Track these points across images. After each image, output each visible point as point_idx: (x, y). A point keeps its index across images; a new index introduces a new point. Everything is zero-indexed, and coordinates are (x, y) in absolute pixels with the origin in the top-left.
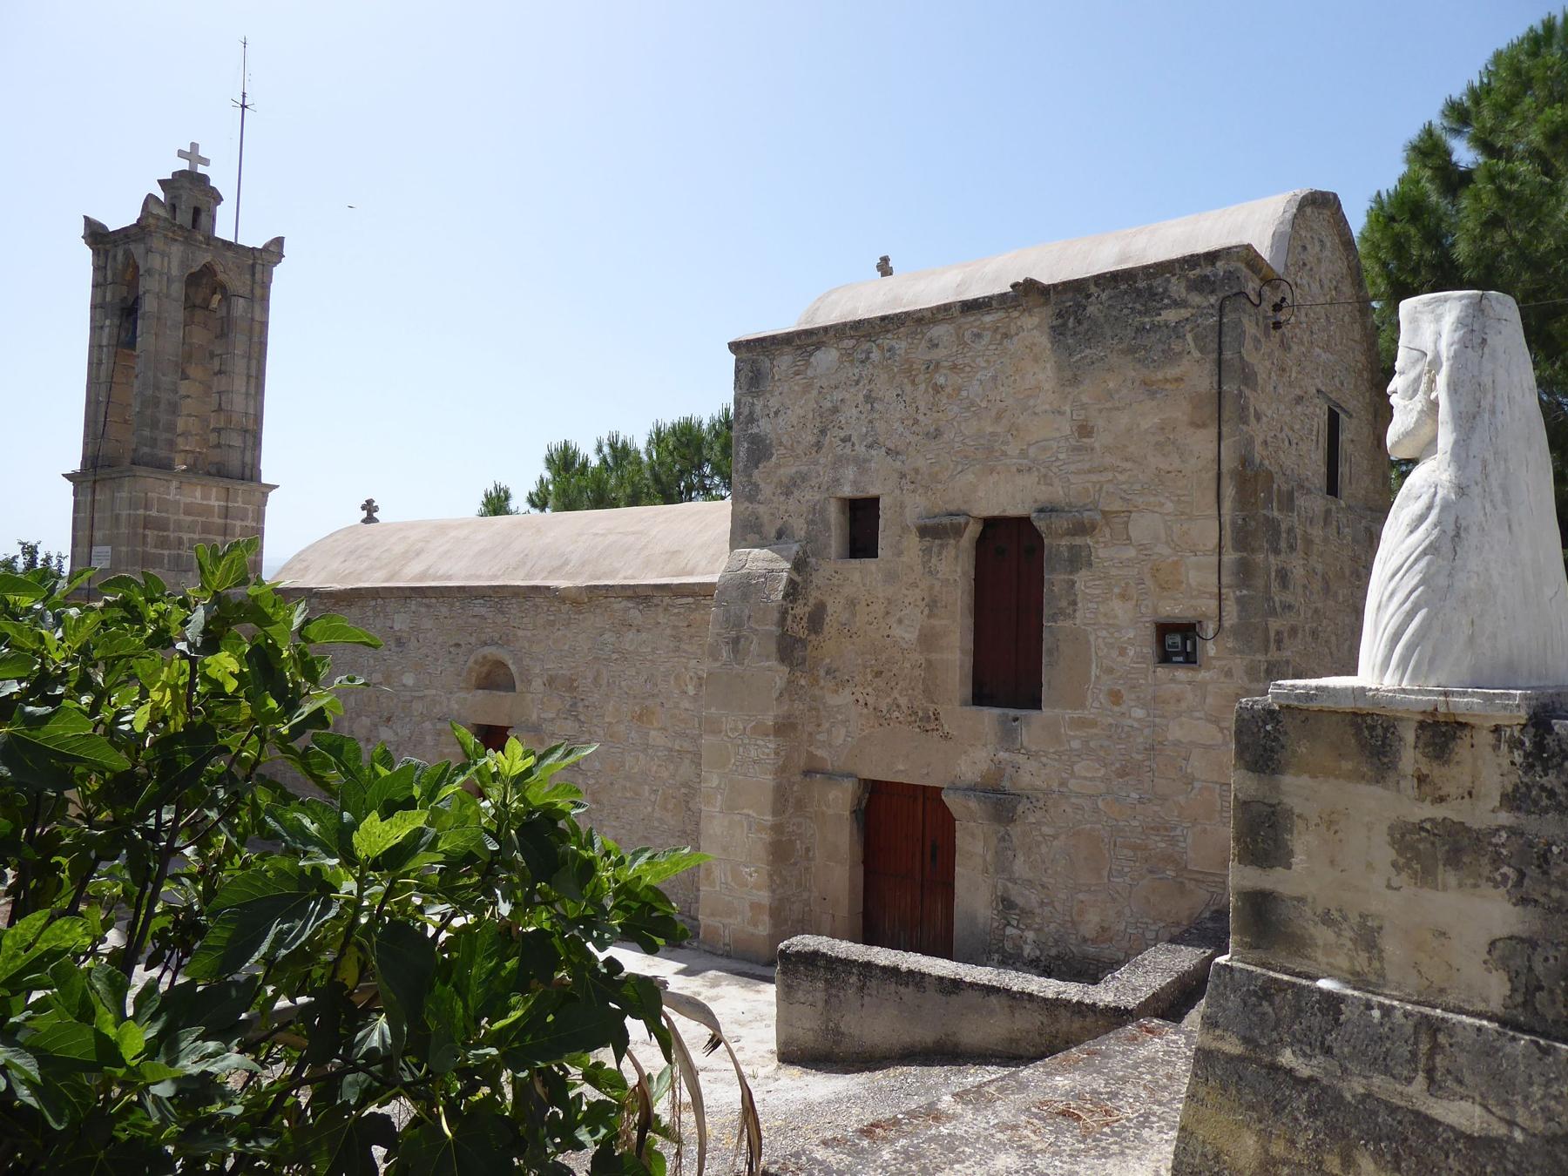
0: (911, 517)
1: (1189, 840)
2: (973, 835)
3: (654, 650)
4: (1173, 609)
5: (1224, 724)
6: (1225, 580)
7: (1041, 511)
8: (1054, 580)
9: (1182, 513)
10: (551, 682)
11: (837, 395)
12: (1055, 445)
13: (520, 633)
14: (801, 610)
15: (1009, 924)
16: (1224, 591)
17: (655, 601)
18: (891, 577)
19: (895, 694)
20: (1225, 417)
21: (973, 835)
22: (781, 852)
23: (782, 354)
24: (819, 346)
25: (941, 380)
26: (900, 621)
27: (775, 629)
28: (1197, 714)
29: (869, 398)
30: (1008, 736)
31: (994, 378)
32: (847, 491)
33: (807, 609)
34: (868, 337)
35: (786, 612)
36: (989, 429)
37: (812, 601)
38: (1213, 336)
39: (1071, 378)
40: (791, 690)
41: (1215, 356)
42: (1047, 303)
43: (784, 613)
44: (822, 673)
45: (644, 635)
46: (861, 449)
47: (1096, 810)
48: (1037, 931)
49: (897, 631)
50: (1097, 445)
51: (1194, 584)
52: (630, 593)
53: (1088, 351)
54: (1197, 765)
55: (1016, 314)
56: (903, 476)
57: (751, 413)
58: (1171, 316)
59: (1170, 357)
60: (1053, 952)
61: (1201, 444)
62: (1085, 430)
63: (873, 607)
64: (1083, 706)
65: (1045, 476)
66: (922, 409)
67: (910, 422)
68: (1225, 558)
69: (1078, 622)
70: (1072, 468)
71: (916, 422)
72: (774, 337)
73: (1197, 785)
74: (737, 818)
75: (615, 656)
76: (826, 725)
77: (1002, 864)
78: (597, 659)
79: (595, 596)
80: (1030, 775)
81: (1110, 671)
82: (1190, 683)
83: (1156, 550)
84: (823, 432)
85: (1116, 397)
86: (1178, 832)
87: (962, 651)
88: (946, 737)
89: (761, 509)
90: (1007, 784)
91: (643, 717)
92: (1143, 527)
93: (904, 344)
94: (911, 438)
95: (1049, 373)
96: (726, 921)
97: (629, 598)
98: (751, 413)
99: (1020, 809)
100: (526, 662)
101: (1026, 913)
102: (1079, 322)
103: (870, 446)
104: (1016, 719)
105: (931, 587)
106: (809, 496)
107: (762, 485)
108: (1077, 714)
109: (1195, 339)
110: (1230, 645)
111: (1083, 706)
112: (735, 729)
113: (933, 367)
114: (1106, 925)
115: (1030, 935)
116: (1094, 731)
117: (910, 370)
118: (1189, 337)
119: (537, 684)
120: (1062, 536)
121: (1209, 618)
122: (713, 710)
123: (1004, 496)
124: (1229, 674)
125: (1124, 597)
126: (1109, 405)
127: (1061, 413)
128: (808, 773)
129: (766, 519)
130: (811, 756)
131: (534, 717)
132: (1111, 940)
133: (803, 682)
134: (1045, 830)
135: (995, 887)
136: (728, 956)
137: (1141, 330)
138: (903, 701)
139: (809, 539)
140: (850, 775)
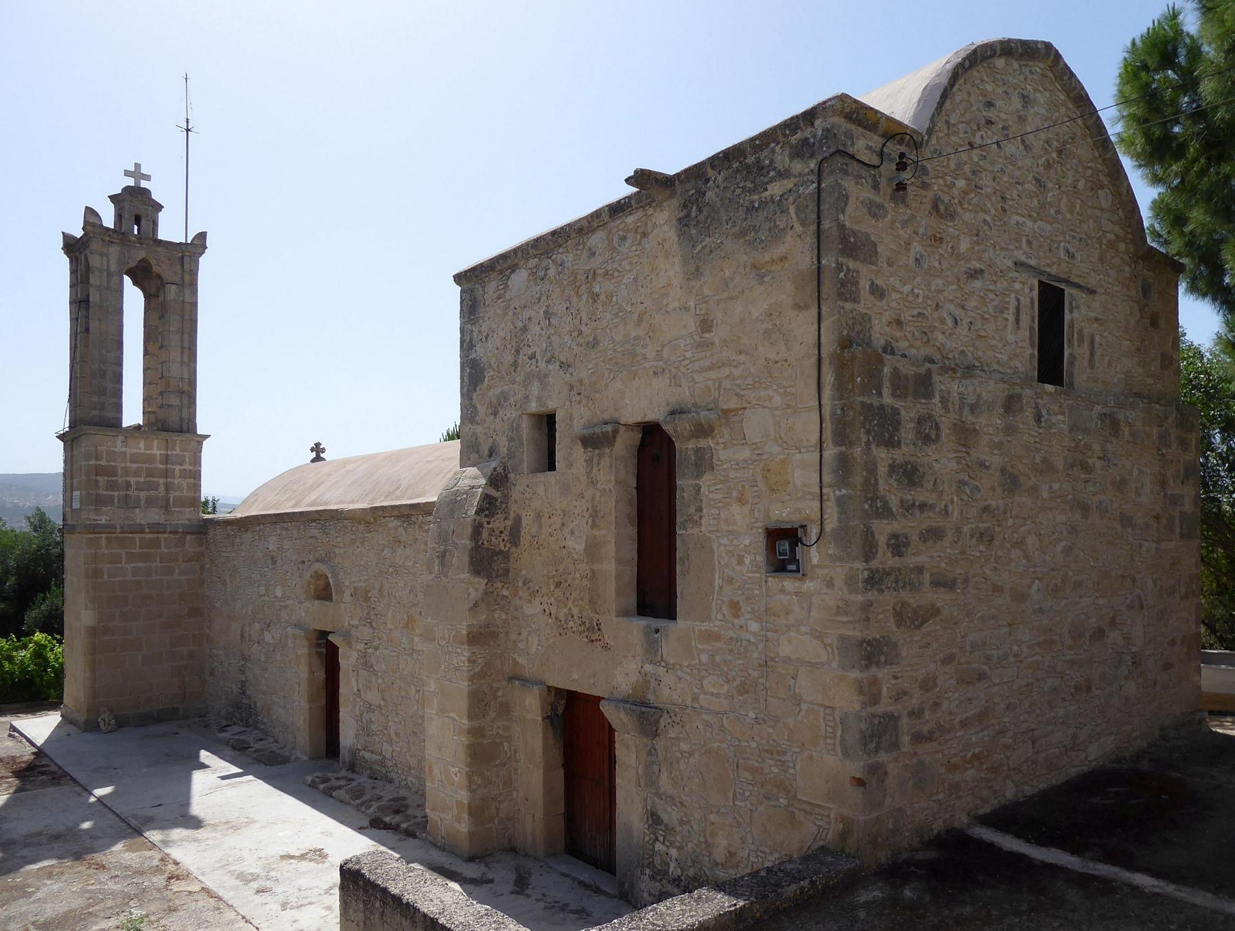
0: (578, 427)
1: (798, 767)
2: (628, 747)
4: (782, 514)
5: (828, 641)
6: (826, 479)
7: (672, 413)
8: (684, 483)
9: (789, 406)
11: (527, 314)
12: (682, 342)
13: (337, 550)
14: (498, 523)
15: (657, 839)
16: (825, 490)
17: (413, 519)
18: (565, 489)
19: (570, 604)
20: (824, 295)
21: (628, 747)
22: (483, 754)
23: (490, 281)
24: (514, 268)
25: (597, 289)
26: (572, 532)
27: (467, 542)
28: (803, 629)
29: (548, 315)
30: (652, 647)
31: (636, 279)
32: (533, 407)
33: (509, 523)
34: (547, 253)
35: (481, 525)
36: (634, 334)
37: (512, 516)
38: (812, 206)
39: (694, 273)
40: (489, 600)
41: (814, 227)
42: (672, 195)
43: (477, 530)
44: (520, 584)
46: (542, 364)
47: (722, 728)
48: (680, 848)
49: (570, 543)
50: (716, 340)
51: (799, 483)
52: (396, 513)
53: (707, 239)
54: (804, 684)
55: (650, 211)
56: (571, 388)
57: (471, 340)
59: (777, 234)
60: (691, 873)
61: (802, 326)
62: (706, 325)
63: (554, 519)
64: (709, 618)
65: (675, 377)
66: (584, 319)
67: (575, 334)
68: (826, 454)
69: (703, 529)
70: (697, 366)
71: (580, 333)
72: (481, 265)
73: (804, 706)
74: (447, 720)
75: (391, 570)
76: (525, 634)
77: (650, 781)
78: (381, 572)
79: (374, 517)
80: (670, 690)
81: (730, 580)
82: (797, 594)
83: (767, 449)
84: (517, 351)
85: (731, 286)
86: (788, 757)
87: (619, 561)
88: (606, 647)
89: (479, 429)
90: (651, 697)
92: (756, 423)
93: (571, 257)
94: (577, 350)
95: (677, 268)
96: (443, 816)
97: (398, 517)
98: (471, 340)
99: (662, 722)
100: (341, 576)
101: (670, 830)
102: (700, 211)
103: (548, 362)
104: (657, 631)
105: (593, 498)
106: (509, 414)
107: (479, 407)
108: (704, 626)
109: (798, 211)
110: (831, 552)
111: (709, 618)
112: (443, 638)
113: (591, 275)
114: (733, 850)
115: (674, 852)
116: (719, 644)
117: (575, 281)
118: (792, 210)
119: (347, 594)
120: (689, 439)
121: (813, 522)
122: (429, 620)
123: (642, 401)
124: (830, 584)
125: (741, 501)
126: (725, 295)
127: (687, 309)
128: (511, 679)
129: (482, 438)
130: (516, 663)
132: (737, 866)
133: (505, 592)
134: (684, 746)
135: (646, 800)
136: (442, 849)
137: (751, 209)
138: (575, 611)
139: (511, 455)
140: (541, 683)
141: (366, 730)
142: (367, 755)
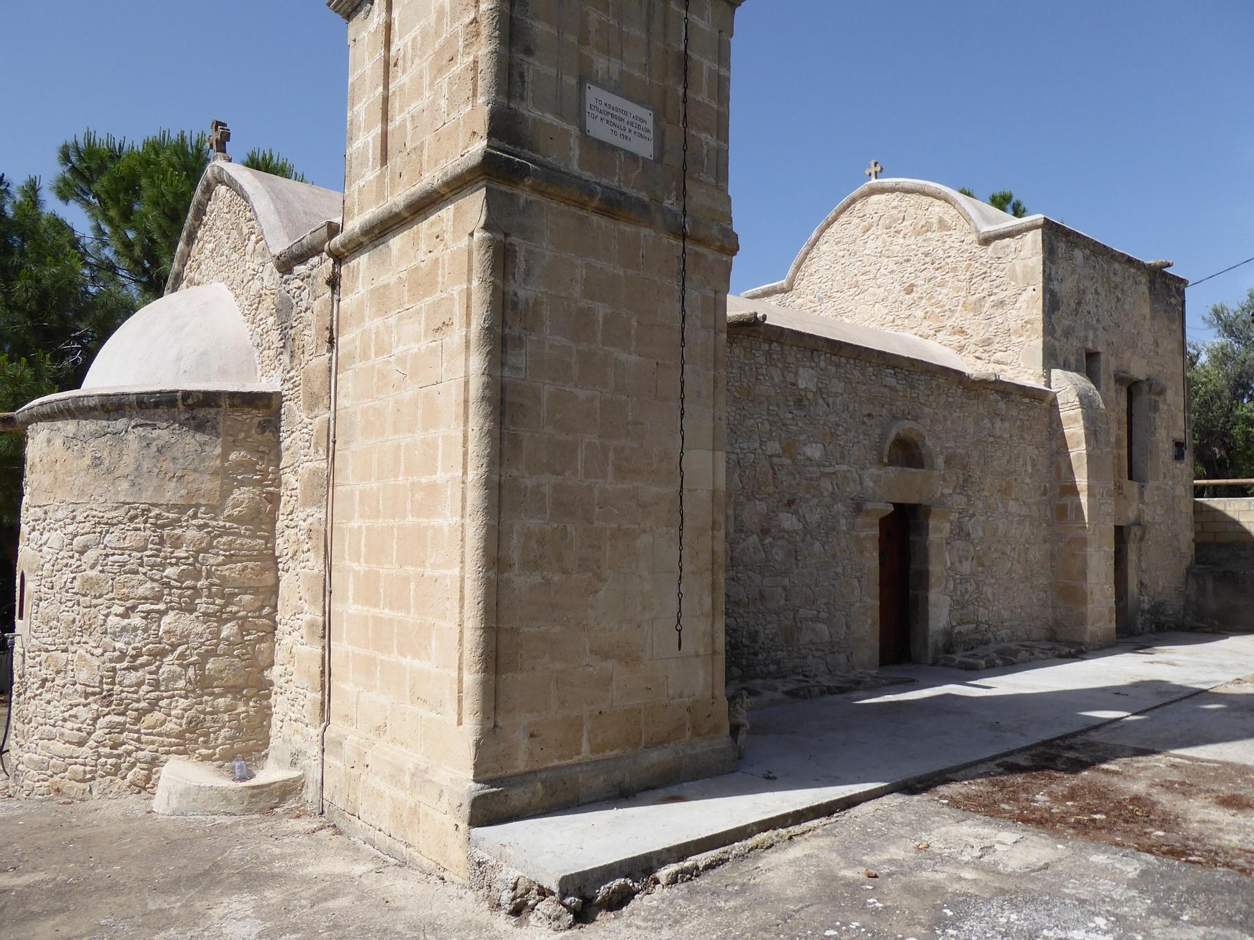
3: (1011, 437)
10: (948, 462)
32: (1090, 345)
45: (1007, 424)
52: (1001, 388)
58: (1173, 301)
75: (991, 439)
80: (1147, 518)
84: (1079, 303)
89: (1057, 344)
91: (1005, 491)
97: (997, 392)
113: (1116, 287)
141: (959, 604)
142: (964, 628)
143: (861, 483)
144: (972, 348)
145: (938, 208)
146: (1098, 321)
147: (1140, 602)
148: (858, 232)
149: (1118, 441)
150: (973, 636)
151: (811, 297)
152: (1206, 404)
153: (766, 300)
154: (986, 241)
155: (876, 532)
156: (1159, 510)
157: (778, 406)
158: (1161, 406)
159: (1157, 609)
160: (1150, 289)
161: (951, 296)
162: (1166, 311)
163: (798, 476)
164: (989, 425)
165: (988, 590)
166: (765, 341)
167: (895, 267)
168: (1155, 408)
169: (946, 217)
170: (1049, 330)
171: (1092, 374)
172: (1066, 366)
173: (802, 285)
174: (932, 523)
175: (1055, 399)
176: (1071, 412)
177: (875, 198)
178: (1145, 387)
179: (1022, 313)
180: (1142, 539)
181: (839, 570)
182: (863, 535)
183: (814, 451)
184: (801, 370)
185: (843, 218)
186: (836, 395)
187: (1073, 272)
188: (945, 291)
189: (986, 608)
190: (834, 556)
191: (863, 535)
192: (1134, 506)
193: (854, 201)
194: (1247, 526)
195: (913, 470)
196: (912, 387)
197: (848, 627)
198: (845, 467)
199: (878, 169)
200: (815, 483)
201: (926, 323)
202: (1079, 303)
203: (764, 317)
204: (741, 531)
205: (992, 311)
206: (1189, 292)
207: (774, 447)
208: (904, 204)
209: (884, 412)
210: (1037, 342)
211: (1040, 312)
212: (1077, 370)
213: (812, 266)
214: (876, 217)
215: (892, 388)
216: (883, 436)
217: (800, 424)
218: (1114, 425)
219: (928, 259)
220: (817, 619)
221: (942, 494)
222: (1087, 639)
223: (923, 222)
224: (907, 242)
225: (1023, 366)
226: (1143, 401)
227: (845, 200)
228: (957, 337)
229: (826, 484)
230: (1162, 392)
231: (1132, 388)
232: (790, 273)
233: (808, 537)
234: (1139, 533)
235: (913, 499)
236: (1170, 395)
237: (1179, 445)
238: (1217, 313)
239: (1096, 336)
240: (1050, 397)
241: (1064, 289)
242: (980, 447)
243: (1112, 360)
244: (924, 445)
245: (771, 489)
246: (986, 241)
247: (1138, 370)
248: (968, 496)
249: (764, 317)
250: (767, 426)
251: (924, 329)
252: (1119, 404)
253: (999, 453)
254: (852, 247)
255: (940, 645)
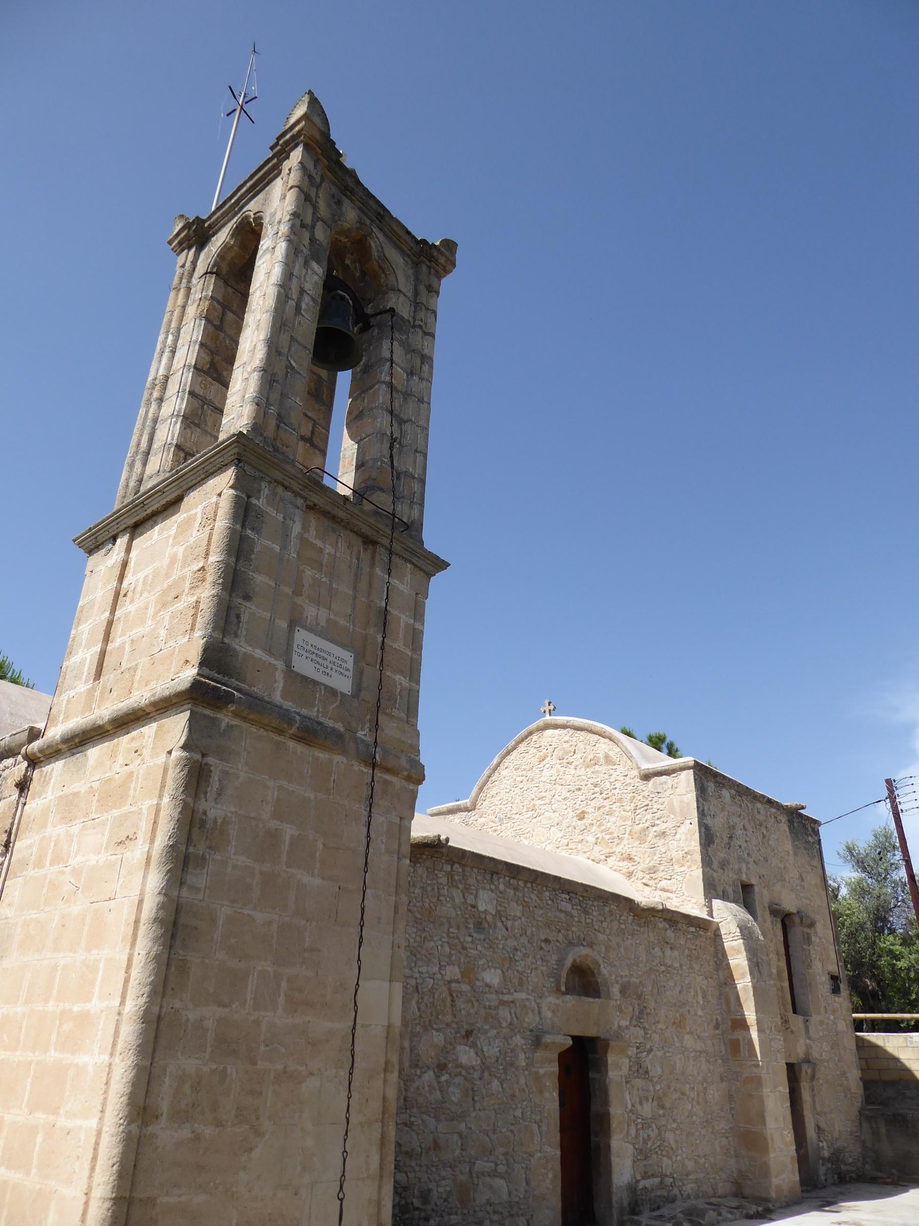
3: (681, 966)
10: (623, 991)
32: (744, 878)
45: (676, 953)
52: (669, 916)
58: (810, 839)
75: (663, 968)
84: (731, 838)
88: (792, 1032)
89: (715, 875)
97: (665, 920)
131: (616, 1025)
141: (642, 1154)
143: (540, 1013)
144: (640, 875)
145: (604, 746)
146: (748, 854)
147: (820, 1149)
148: (535, 760)
149: (779, 972)
150: (659, 1193)
151: (493, 817)
152: (852, 935)
153: (451, 817)
154: (646, 777)
155: (555, 1068)
156: (826, 1047)
157: (458, 928)
158: (813, 938)
159: (836, 1158)
160: (789, 827)
161: (618, 824)
162: (806, 849)
163: (476, 1004)
164: (660, 954)
165: (670, 1137)
166: (447, 862)
167: (568, 795)
168: (808, 940)
169: (611, 754)
170: (707, 862)
171: (748, 905)
172: (724, 897)
173: (484, 805)
174: (611, 1058)
175: (718, 929)
176: (734, 943)
177: (549, 732)
178: (797, 920)
179: (682, 844)
180: (813, 1078)
181: (518, 1113)
182: (542, 1071)
183: (492, 977)
184: (481, 892)
185: (522, 747)
186: (514, 919)
187: (723, 809)
188: (613, 819)
189: (669, 1158)
190: (513, 1096)
191: (542, 1071)
192: (802, 1041)
193: (531, 733)
194: (908, 1064)
195: (591, 1000)
196: (586, 913)
197: (528, 1183)
198: (523, 996)
199: (552, 707)
200: (493, 1012)
201: (597, 848)
202: (731, 838)
203: (447, 840)
204: (417, 1066)
205: (655, 840)
206: (821, 829)
207: (453, 972)
208: (575, 739)
209: (560, 937)
210: (697, 873)
211: (698, 844)
212: (735, 901)
213: (493, 789)
214: (551, 749)
215: (566, 913)
216: (560, 962)
217: (479, 948)
218: (773, 956)
219: (597, 789)
220: (494, 1174)
221: (619, 1027)
222: (773, 1195)
223: (591, 757)
224: (578, 773)
225: (685, 894)
226: (797, 932)
227: (523, 732)
228: (625, 863)
229: (504, 1014)
230: (812, 925)
231: (786, 920)
232: (473, 794)
233: (486, 1074)
234: (809, 1071)
235: (591, 1032)
236: (819, 927)
237: (834, 978)
238: (850, 850)
239: (748, 869)
240: (714, 927)
241: (717, 823)
242: (653, 976)
243: (765, 892)
244: (600, 973)
245: (449, 1018)
246: (646, 777)
247: (789, 903)
248: (644, 1028)
249: (447, 840)
250: (447, 949)
251: (595, 854)
252: (775, 935)
253: (671, 984)
254: (529, 774)
255: (625, 1204)
